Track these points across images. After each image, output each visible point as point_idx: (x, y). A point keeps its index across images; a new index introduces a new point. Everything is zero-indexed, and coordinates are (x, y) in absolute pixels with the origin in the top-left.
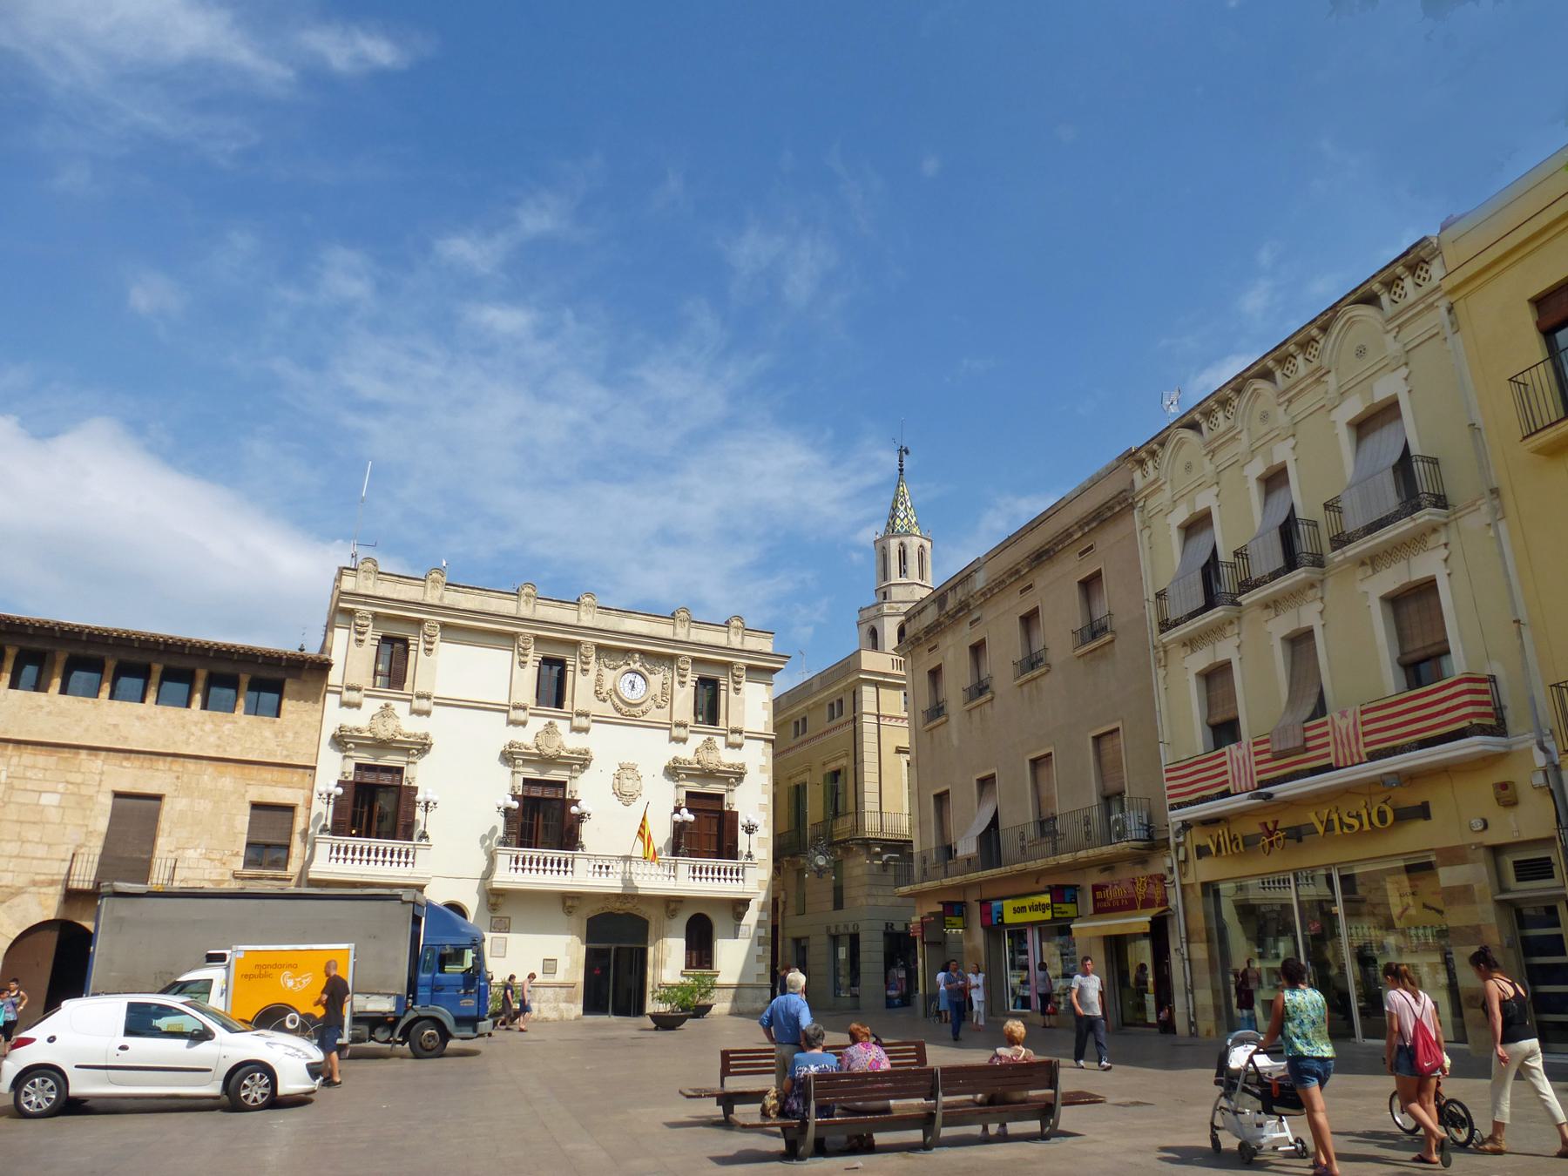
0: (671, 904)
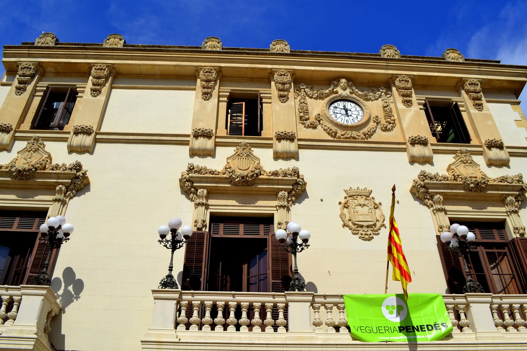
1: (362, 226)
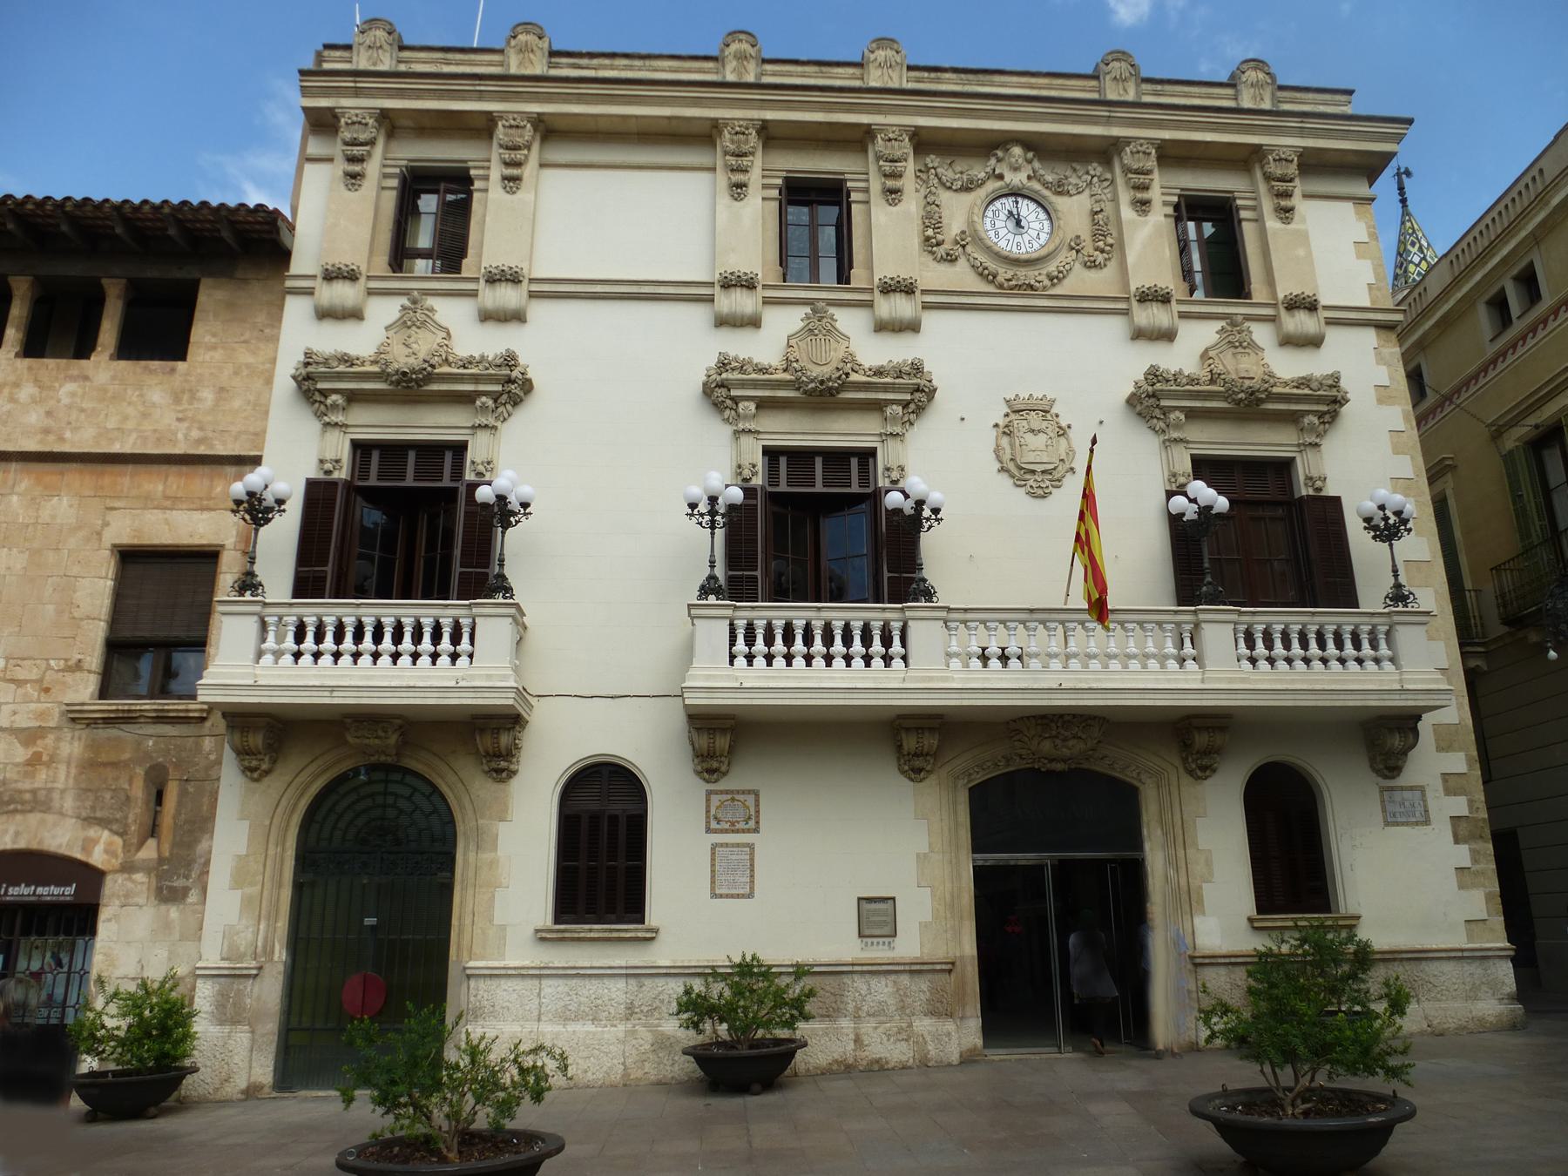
0: (1194, 735)
1: (1033, 472)
